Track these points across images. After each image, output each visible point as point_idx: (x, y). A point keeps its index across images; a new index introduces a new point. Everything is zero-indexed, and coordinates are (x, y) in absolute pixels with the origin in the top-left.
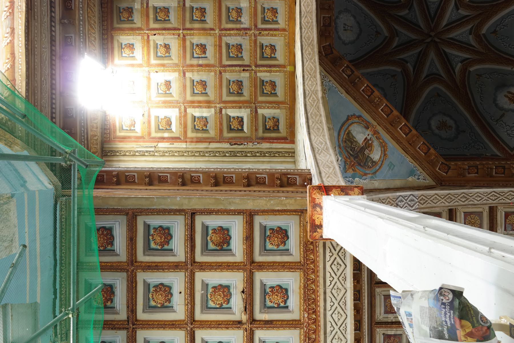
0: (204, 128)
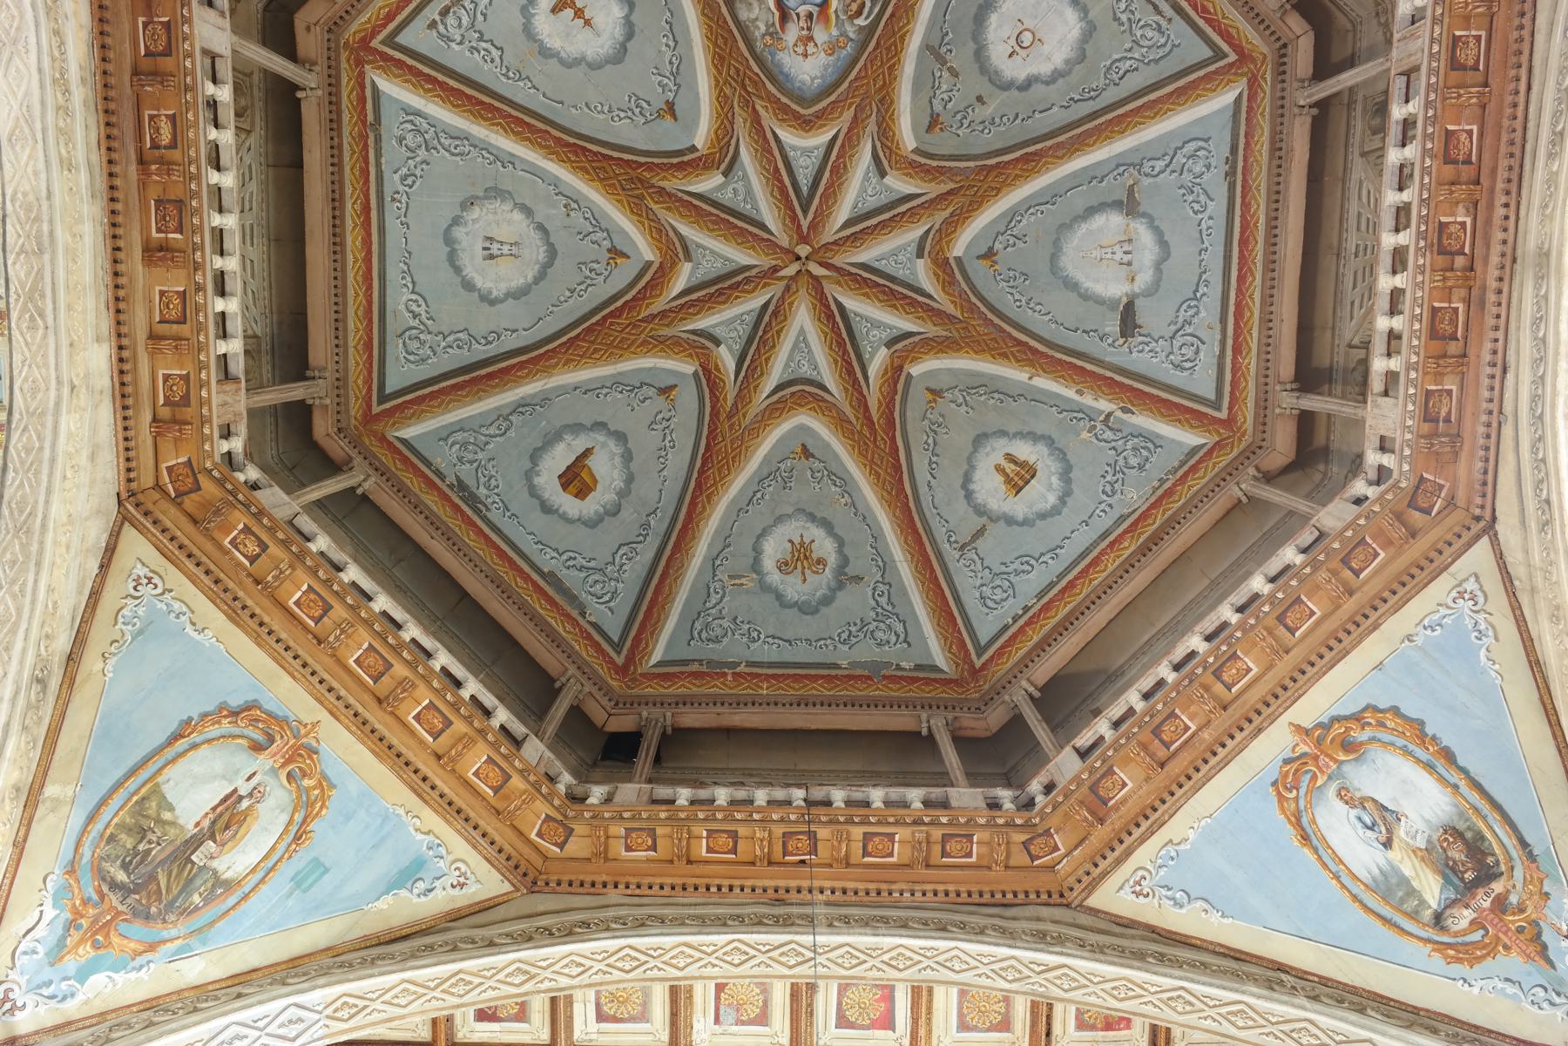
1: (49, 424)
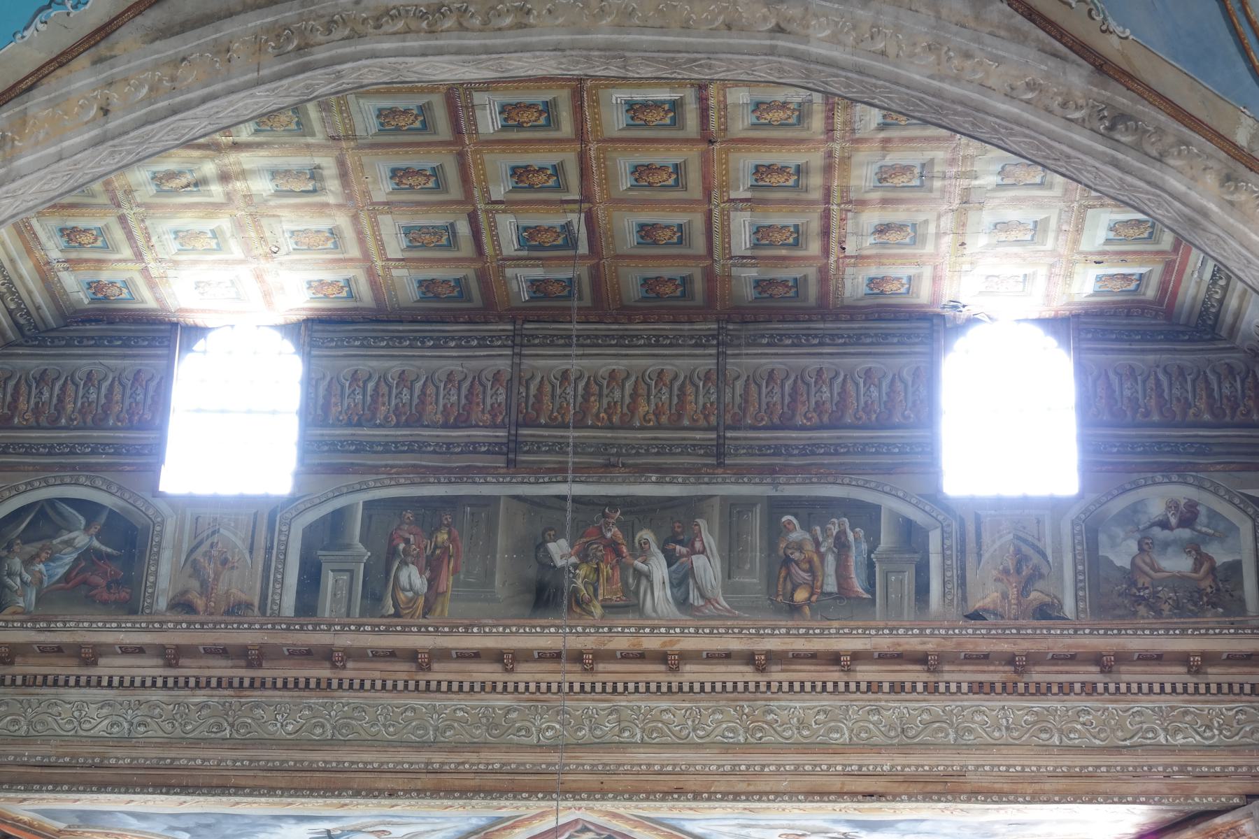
1: (819, 67)
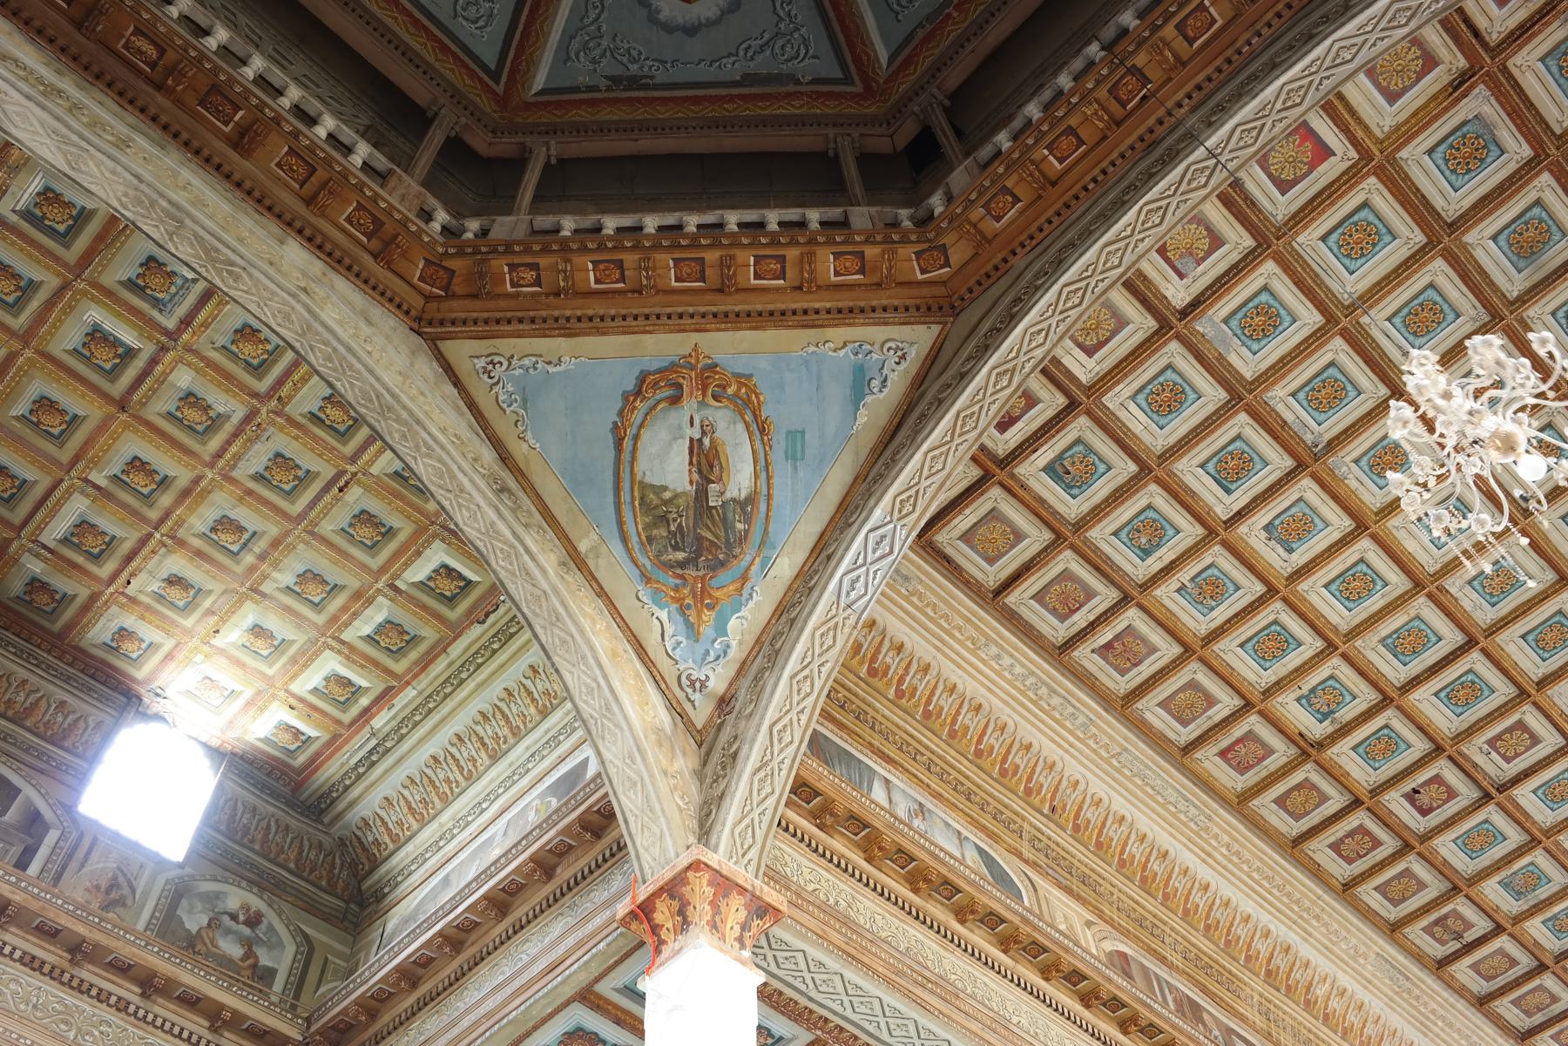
0: (407, 638)
1: (320, 329)
